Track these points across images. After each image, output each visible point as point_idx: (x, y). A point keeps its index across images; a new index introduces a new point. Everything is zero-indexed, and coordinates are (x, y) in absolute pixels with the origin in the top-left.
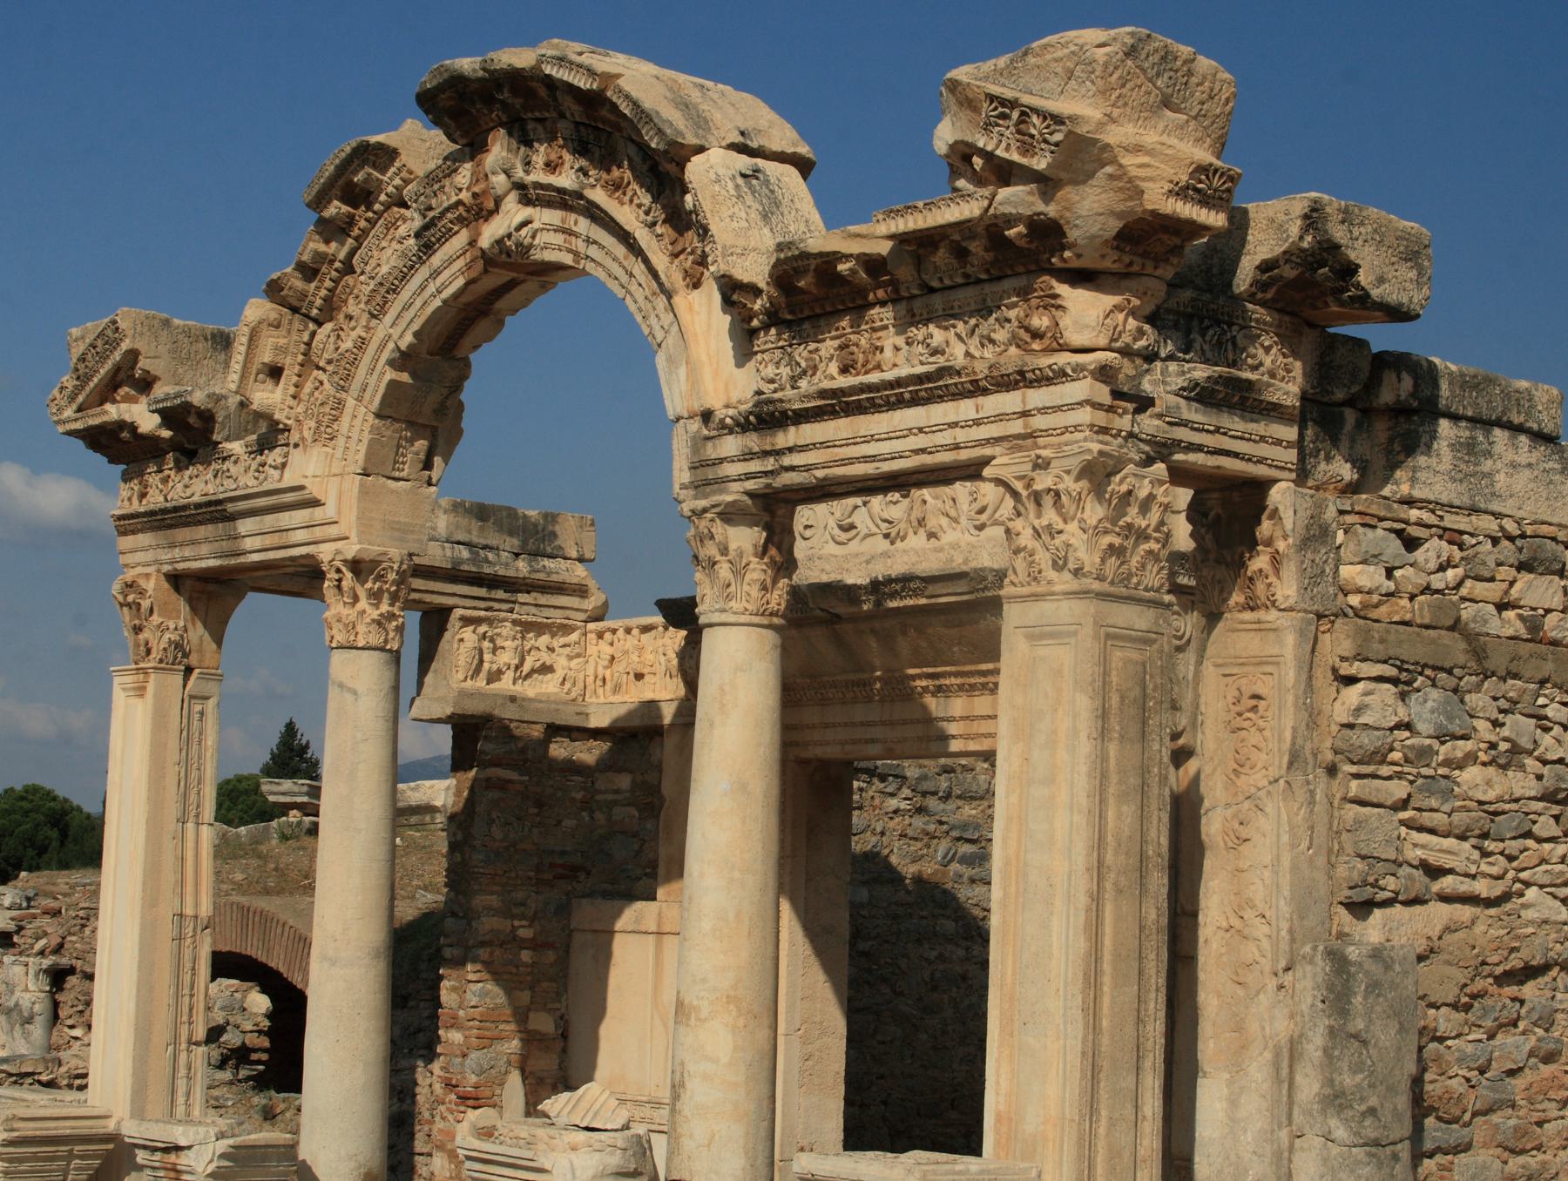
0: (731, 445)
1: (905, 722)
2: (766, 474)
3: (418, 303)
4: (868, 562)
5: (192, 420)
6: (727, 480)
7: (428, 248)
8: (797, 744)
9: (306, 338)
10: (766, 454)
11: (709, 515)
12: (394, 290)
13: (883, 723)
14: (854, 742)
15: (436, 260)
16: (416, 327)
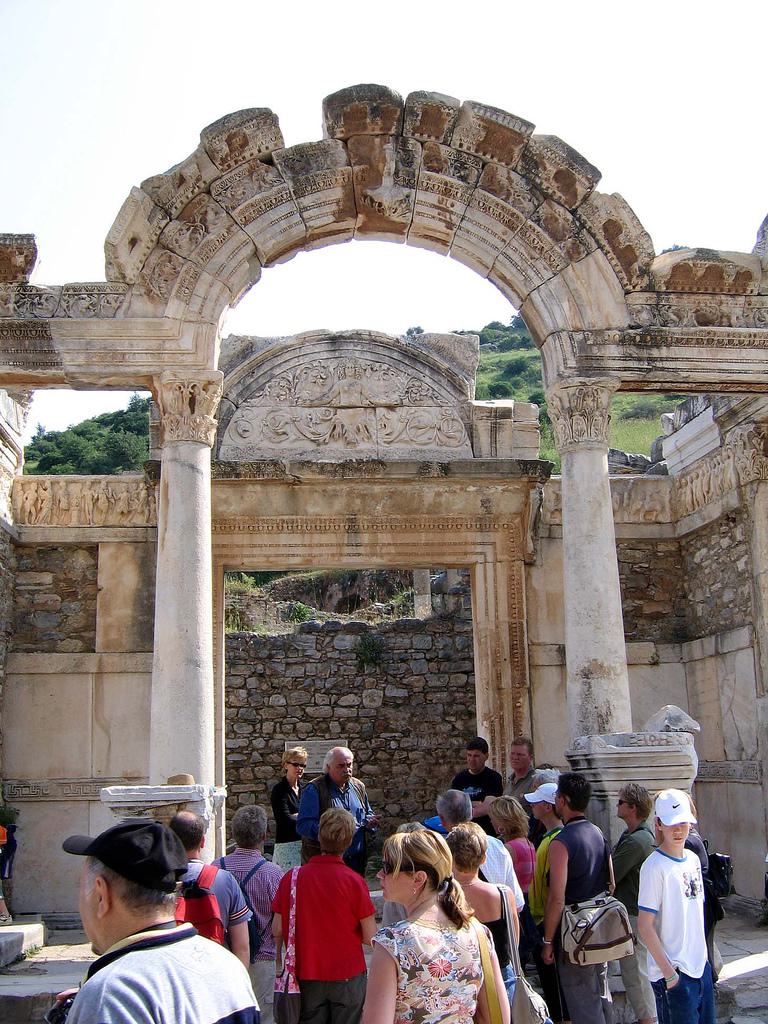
0: (613, 351)
1: (321, 545)
2: (640, 370)
3: (284, 224)
4: (301, 454)
5: (20, 260)
6: (610, 369)
7: (299, 193)
8: (227, 556)
9: (162, 226)
10: (639, 359)
11: (595, 387)
12: (260, 213)
13: (305, 546)
14: (277, 556)
15: (306, 201)
16: (280, 238)
